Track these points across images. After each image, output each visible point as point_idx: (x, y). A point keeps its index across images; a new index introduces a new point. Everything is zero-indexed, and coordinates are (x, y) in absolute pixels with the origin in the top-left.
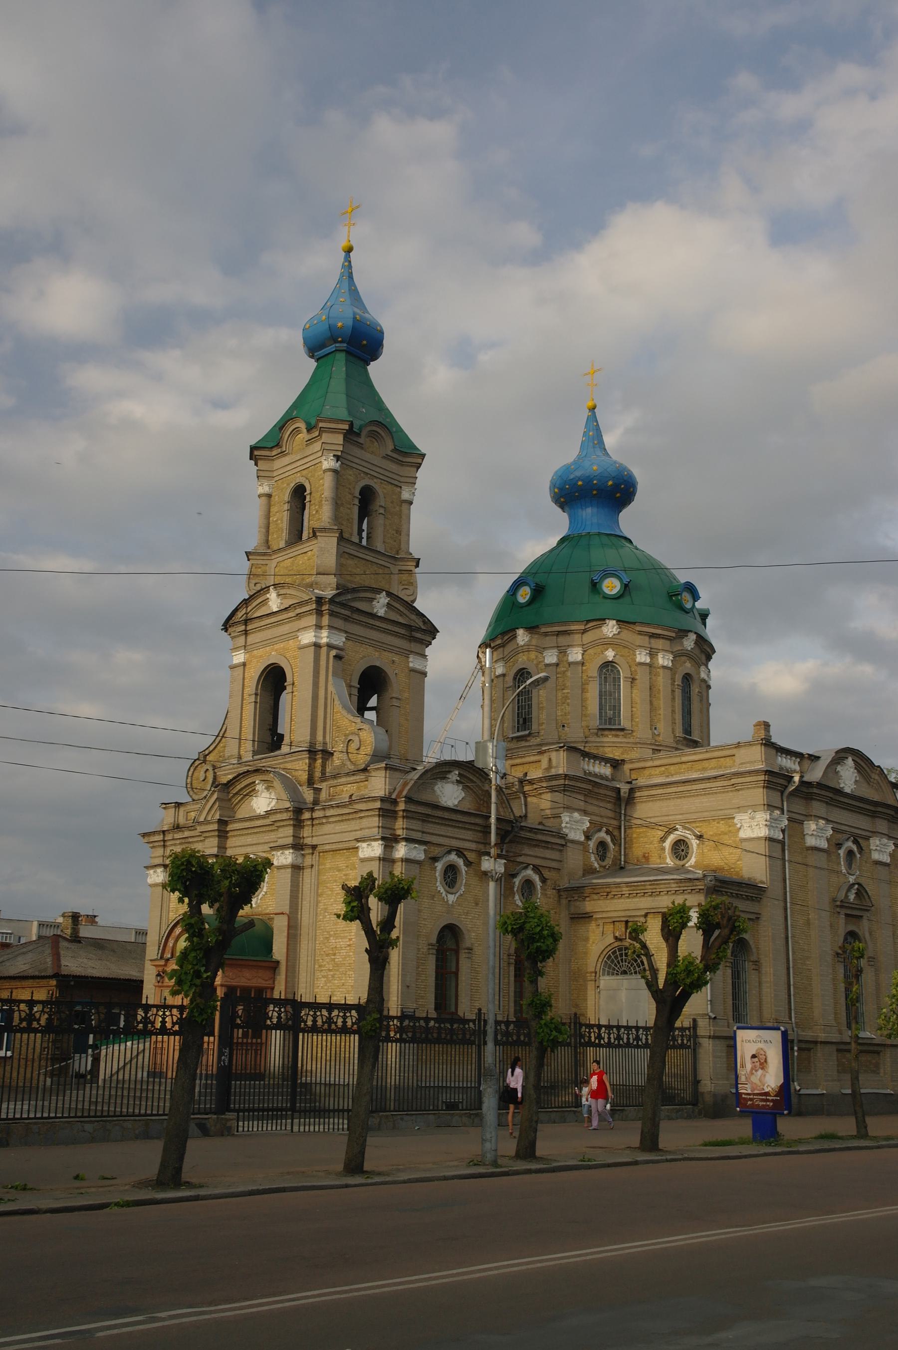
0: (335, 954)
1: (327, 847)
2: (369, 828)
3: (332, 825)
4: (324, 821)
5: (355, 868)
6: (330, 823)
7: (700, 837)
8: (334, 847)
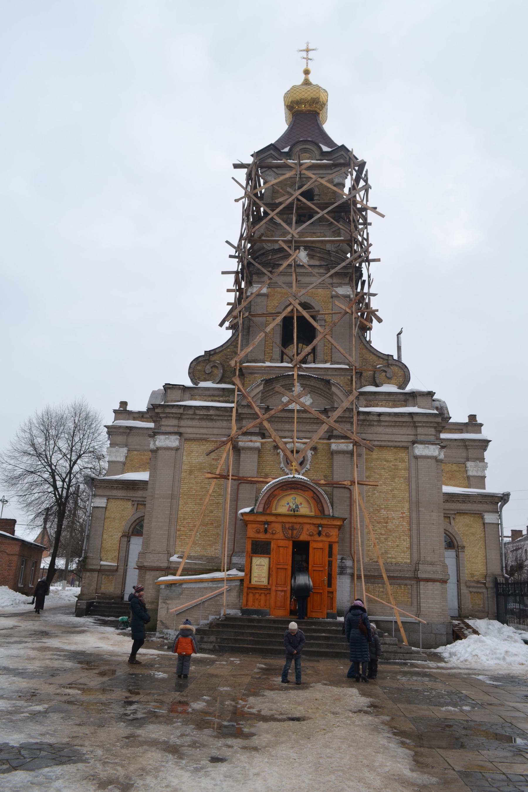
0: (387, 523)
1: (376, 443)
2: (426, 435)
3: (382, 428)
4: (376, 423)
5: (404, 461)
6: (380, 426)
8: (383, 443)
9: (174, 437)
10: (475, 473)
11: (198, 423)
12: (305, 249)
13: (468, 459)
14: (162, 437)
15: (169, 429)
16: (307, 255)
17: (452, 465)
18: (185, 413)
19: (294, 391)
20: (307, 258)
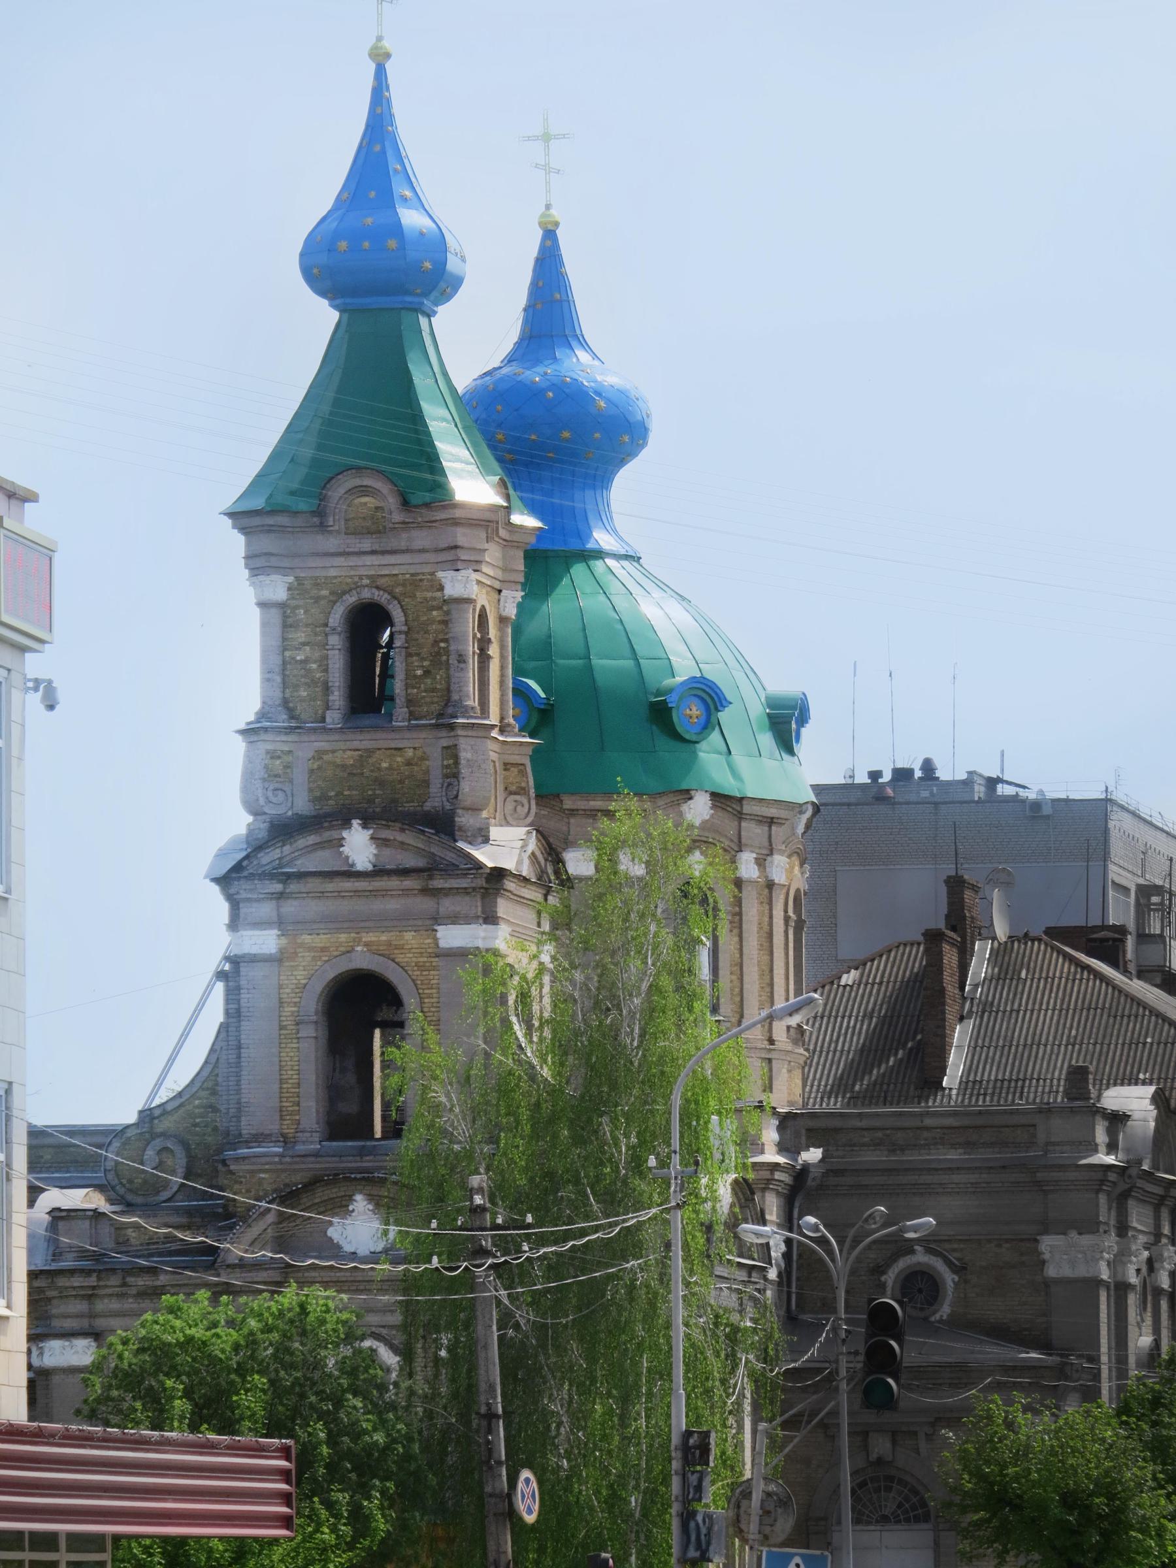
7: (959, 1269)
9: (81, 1343)
10: (1067, 1272)
11: (135, 1306)
12: (365, 826)
13: (1047, 1228)
14: (56, 1344)
15: (69, 1324)
16: (372, 838)
17: (999, 1246)
18: (101, 1283)
19: (353, 1211)
20: (373, 850)
